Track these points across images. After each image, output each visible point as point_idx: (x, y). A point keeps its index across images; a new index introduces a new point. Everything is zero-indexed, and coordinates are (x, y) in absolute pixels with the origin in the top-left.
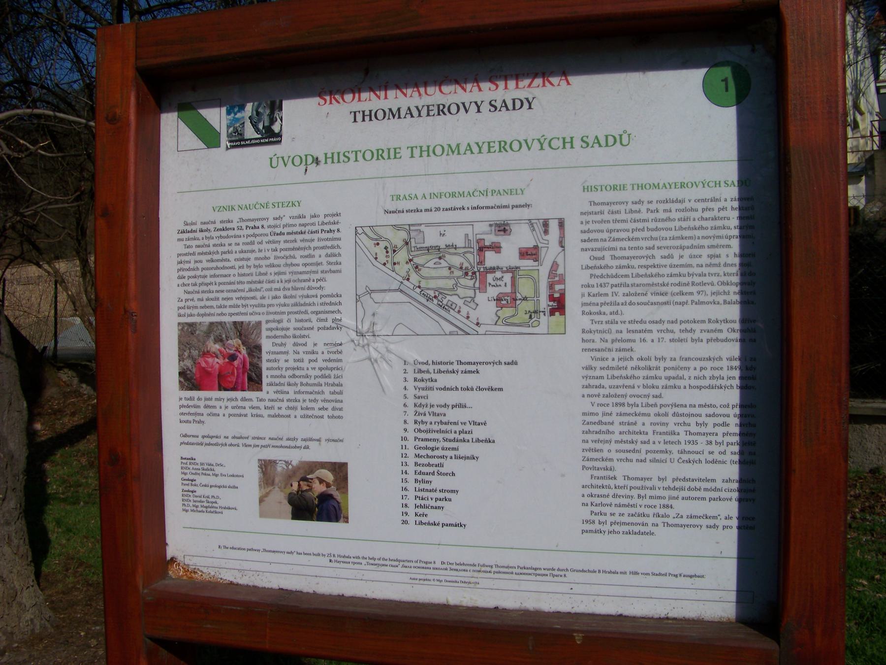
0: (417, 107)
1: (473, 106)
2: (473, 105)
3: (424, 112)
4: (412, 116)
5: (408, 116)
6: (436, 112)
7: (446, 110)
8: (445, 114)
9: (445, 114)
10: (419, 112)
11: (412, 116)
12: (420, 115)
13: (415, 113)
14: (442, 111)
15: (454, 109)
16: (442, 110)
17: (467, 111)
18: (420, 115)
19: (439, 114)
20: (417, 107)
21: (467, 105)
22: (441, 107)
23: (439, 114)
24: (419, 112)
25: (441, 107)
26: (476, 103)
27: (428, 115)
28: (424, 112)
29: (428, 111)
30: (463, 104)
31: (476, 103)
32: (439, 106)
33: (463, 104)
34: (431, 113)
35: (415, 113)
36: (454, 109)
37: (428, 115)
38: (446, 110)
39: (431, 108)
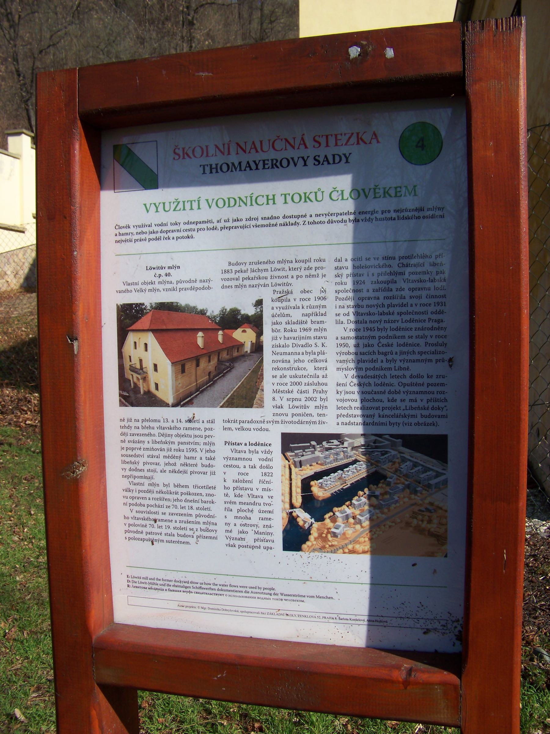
0: (255, 162)
1: (301, 161)
2: (301, 159)
3: (261, 166)
4: (251, 169)
5: (248, 169)
6: (270, 165)
7: (278, 164)
8: (278, 167)
9: (278, 167)
10: (257, 165)
11: (251, 169)
12: (257, 169)
13: (253, 166)
14: (276, 165)
15: (285, 163)
17: (295, 165)
18: (257, 169)
19: (273, 167)
20: (255, 162)
21: (296, 160)
22: (275, 162)
24: (257, 165)
25: (275, 162)
26: (303, 158)
27: (264, 168)
28: (261, 166)
29: (264, 165)
30: (292, 159)
31: (303, 158)
32: (272, 160)
33: (292, 159)
34: (266, 167)
35: (253, 166)
36: (285, 163)
37: (264, 168)
38: (278, 164)
39: (266, 162)
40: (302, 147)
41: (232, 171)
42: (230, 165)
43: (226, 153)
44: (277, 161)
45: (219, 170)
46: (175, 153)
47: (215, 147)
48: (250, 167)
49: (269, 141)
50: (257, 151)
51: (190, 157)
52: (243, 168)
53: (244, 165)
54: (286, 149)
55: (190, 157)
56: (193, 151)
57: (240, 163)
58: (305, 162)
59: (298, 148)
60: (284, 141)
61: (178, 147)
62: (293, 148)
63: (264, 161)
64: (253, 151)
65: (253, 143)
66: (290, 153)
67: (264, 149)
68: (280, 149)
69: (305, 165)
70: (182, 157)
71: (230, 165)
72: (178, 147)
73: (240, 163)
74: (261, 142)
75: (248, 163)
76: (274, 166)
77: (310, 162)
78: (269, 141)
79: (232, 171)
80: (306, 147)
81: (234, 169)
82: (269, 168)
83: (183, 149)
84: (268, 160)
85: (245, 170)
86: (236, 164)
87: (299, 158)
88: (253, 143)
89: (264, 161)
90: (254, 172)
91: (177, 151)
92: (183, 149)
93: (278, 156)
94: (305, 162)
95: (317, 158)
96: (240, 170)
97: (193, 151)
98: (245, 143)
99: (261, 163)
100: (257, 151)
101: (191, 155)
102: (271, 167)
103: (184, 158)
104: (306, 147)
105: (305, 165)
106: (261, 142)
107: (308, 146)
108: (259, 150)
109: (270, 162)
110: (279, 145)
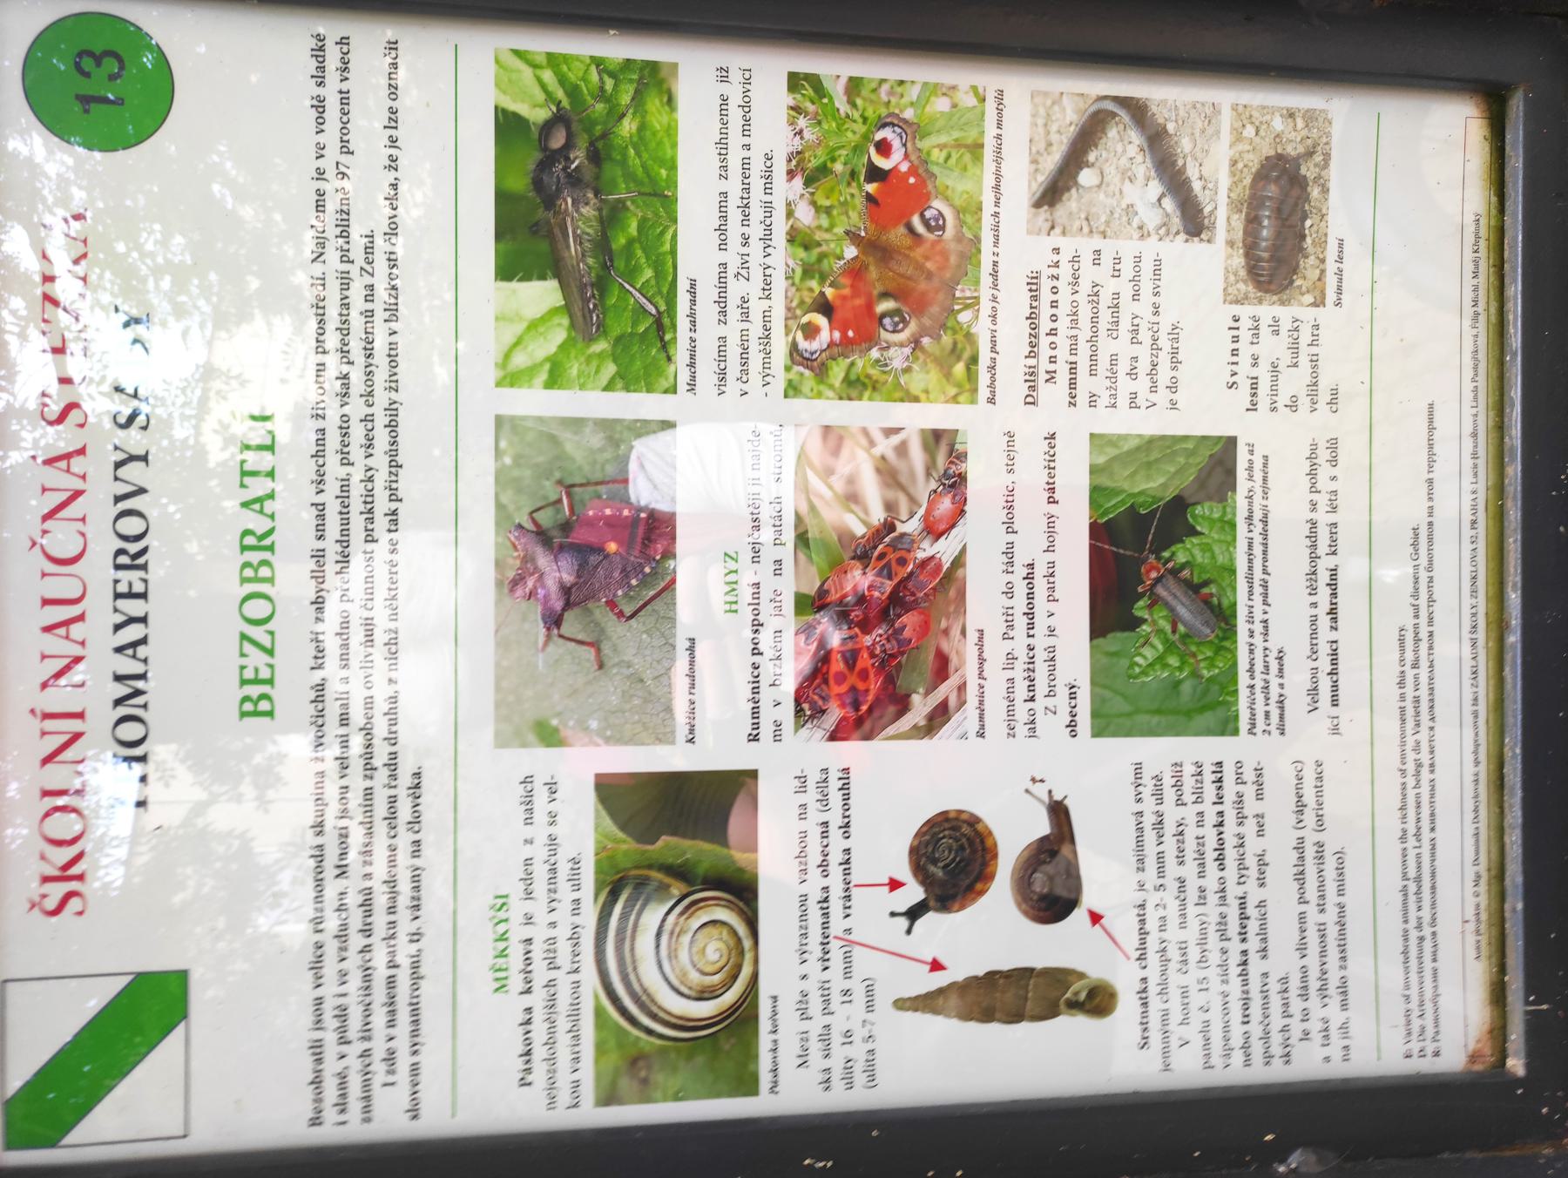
0: (118, 627)
2: (123, 472)
3: (134, 607)
4: (143, 641)
5: (142, 651)
6: (134, 576)
7: (133, 548)
8: (144, 551)
9: (144, 551)
10: (132, 620)
11: (143, 641)
12: (143, 620)
13: (133, 633)
15: (131, 526)
16: (131, 556)
17: (142, 491)
18: (143, 620)
19: (144, 567)
20: (118, 627)
22: (123, 560)
23: (144, 567)
24: (132, 620)
25: (123, 560)
26: (118, 465)
27: (143, 596)
28: (134, 607)
29: (131, 595)
30: (118, 499)
31: (118, 465)
32: (118, 567)
34: (138, 587)
35: (133, 633)
36: (131, 526)
38: (133, 548)
39: (122, 588)
40: (77, 464)
41: (145, 706)
42: (123, 711)
43: (74, 725)
44: (120, 552)
45: (138, 751)
46: (56, 912)
47: (49, 766)
48: (134, 645)
49: (44, 575)
50: (81, 618)
51: (79, 857)
52: (138, 668)
53: (128, 666)
54: (83, 520)
55: (79, 857)
56: (59, 843)
57: (119, 678)
58: (133, 458)
59: (84, 477)
60: (49, 525)
61: (37, 899)
62: (78, 494)
63: (118, 596)
64: (77, 630)
65: (48, 629)
66: (98, 505)
67: (77, 594)
68: (81, 540)
69: (144, 458)
70: (73, 886)
71: (123, 711)
72: (37, 899)
73: (119, 678)
74: (46, 602)
75: (119, 650)
76: (141, 561)
77: (134, 440)
78: (44, 575)
79: (145, 706)
80: (82, 451)
81: (139, 700)
82: (145, 581)
83: (46, 879)
84: (116, 582)
85: (145, 661)
86: (127, 691)
87: (116, 479)
88: (48, 629)
89: (118, 596)
90: (154, 630)
91: (51, 904)
92: (46, 879)
93: (104, 545)
94: (133, 458)
95: (122, 420)
96: (143, 677)
97: (59, 843)
98: (44, 657)
99: (121, 603)
100: (81, 618)
101: (68, 853)
102: (141, 574)
103: (80, 878)
104: (82, 451)
105: (144, 458)
106: (46, 602)
107: (79, 446)
108: (74, 611)
109: (124, 575)
110: (63, 540)
